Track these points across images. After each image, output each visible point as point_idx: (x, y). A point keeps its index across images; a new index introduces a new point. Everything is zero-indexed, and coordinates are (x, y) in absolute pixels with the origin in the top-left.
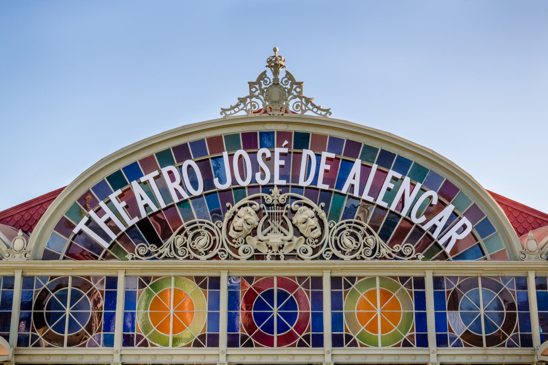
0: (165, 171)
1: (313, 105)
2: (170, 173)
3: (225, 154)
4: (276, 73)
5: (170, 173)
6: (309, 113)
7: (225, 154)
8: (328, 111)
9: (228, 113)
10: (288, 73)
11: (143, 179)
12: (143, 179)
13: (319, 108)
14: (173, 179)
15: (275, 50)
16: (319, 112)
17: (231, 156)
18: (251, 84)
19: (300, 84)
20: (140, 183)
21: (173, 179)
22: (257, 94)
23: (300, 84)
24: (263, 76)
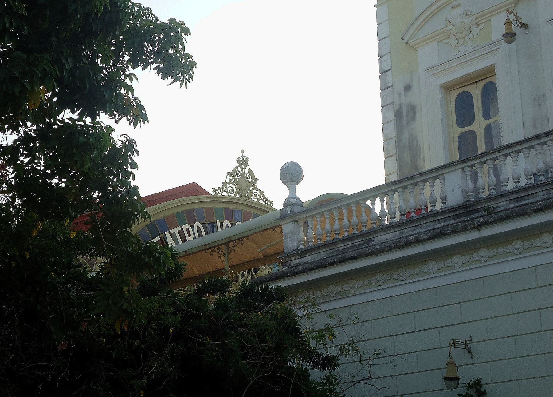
0: (185, 227)
1: (264, 197)
2: (187, 229)
3: (218, 222)
4: (243, 169)
5: (187, 229)
6: (261, 201)
7: (218, 222)
8: (271, 202)
9: (217, 192)
10: (250, 171)
11: (172, 231)
12: (172, 231)
13: (267, 199)
14: (190, 235)
15: (242, 152)
16: (267, 202)
17: (221, 224)
18: (228, 173)
19: (256, 180)
20: (170, 233)
21: (190, 235)
22: (233, 181)
23: (256, 180)
24: (236, 169)
